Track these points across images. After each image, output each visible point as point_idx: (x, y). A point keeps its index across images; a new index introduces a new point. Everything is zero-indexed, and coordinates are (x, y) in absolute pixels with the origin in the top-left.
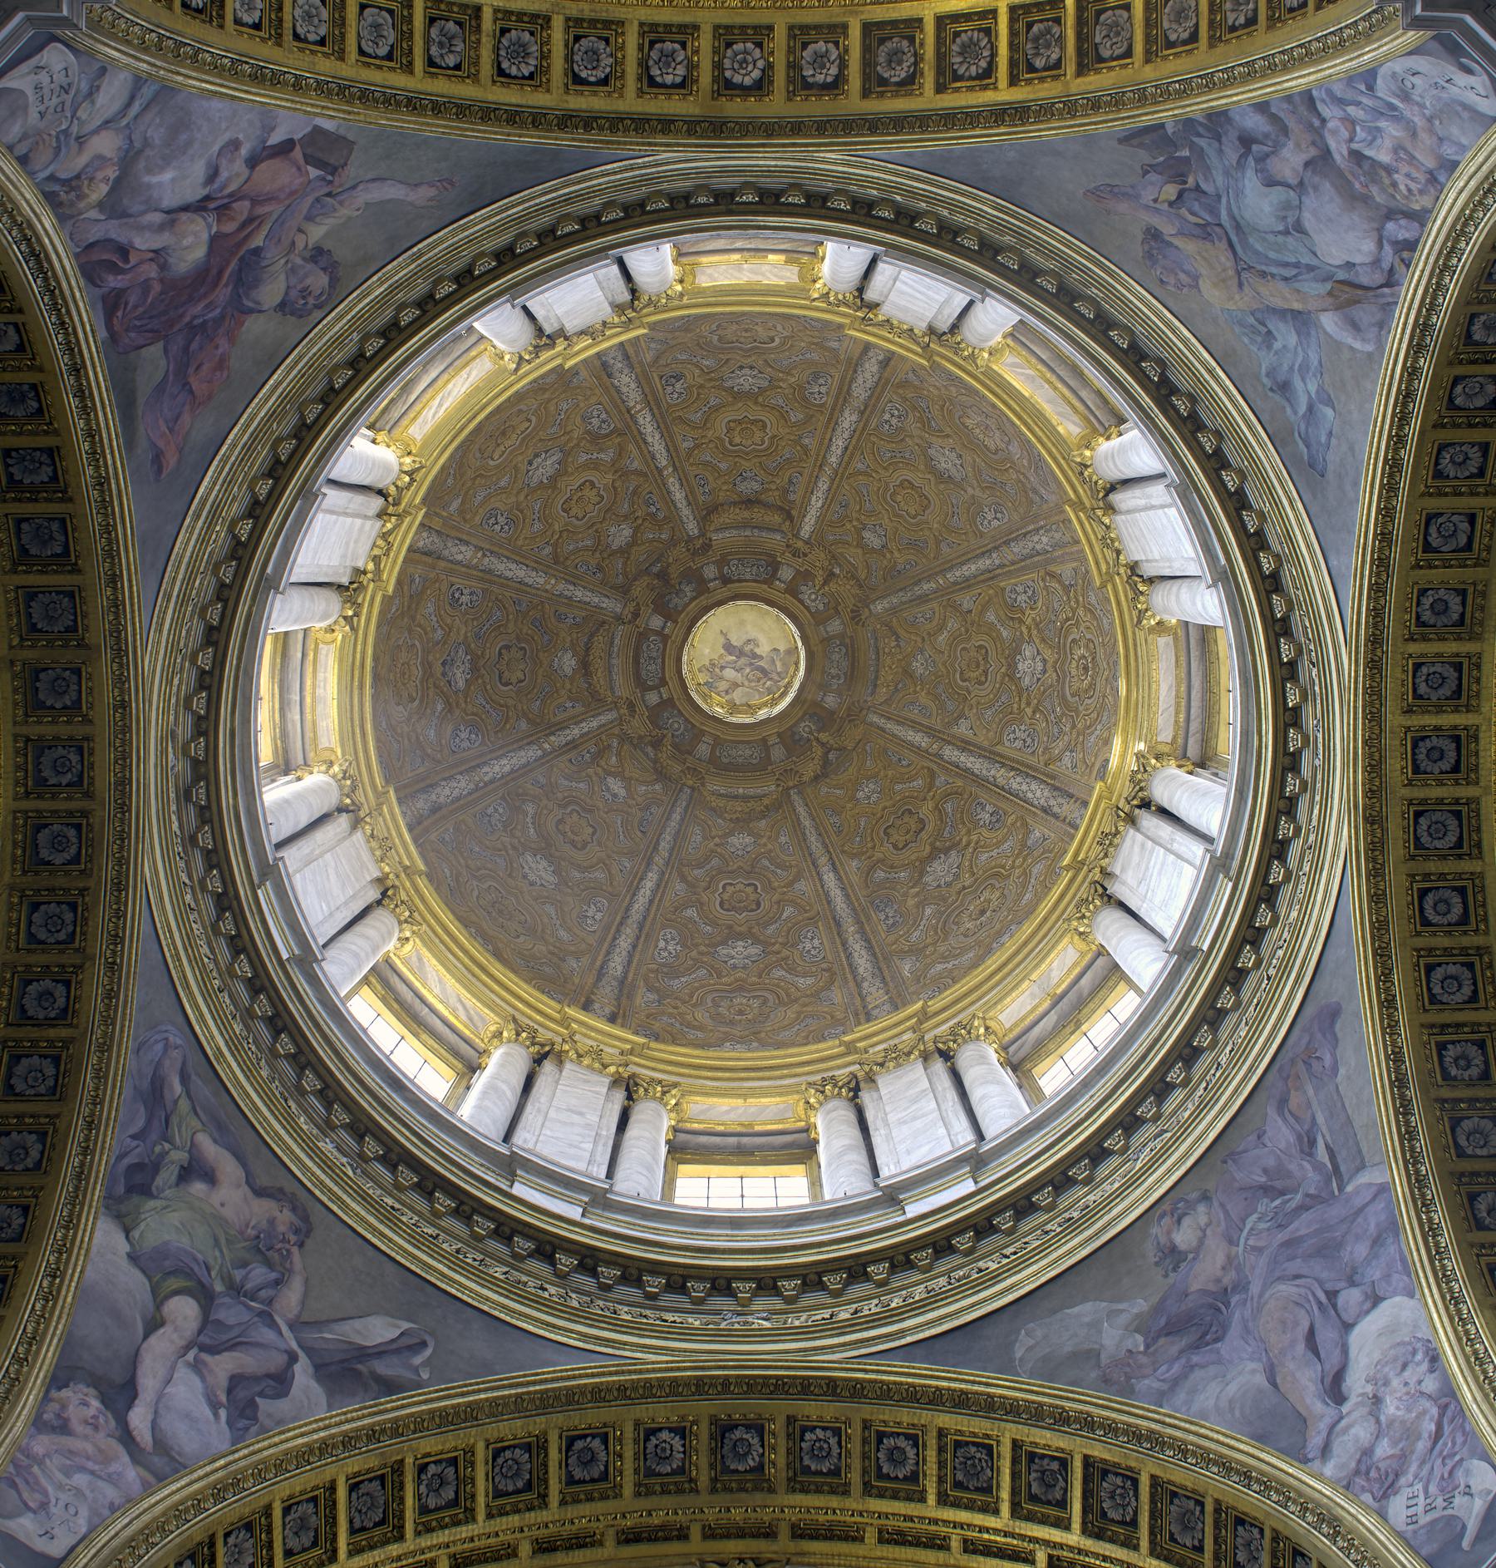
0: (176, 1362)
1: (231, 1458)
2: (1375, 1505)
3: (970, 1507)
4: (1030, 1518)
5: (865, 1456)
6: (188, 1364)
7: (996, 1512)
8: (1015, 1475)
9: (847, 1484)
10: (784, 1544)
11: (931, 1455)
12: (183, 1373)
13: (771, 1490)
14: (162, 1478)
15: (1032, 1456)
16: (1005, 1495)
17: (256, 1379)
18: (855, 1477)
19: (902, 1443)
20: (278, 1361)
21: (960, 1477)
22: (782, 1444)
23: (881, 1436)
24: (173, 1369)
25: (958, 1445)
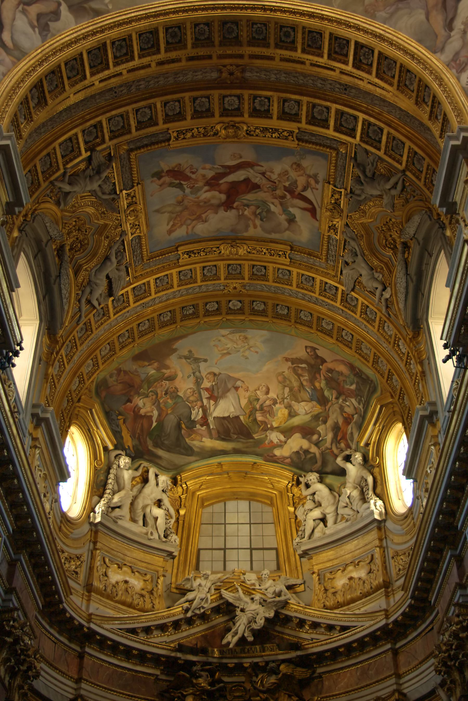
0: (15, 11)
1: (42, 48)
2: (457, 75)
3: (313, 54)
4: (335, 60)
5: (275, 34)
6: (20, 11)
7: (322, 57)
8: (330, 44)
9: (269, 44)
10: (246, 60)
11: (300, 36)
12: (19, 15)
13: (241, 46)
14: (19, 59)
15: (336, 38)
16: (326, 51)
17: (47, 14)
18: (272, 42)
19: (289, 30)
20: (52, 7)
21: (310, 43)
22: (245, 29)
23: (282, 27)
24: (15, 14)
25: (310, 32)
